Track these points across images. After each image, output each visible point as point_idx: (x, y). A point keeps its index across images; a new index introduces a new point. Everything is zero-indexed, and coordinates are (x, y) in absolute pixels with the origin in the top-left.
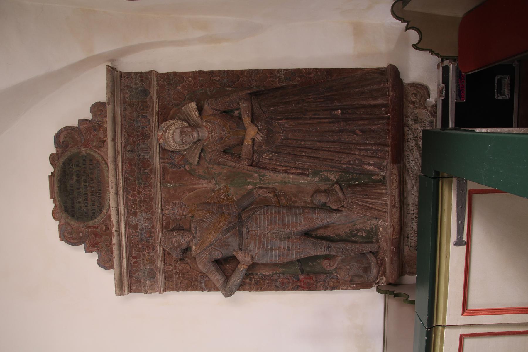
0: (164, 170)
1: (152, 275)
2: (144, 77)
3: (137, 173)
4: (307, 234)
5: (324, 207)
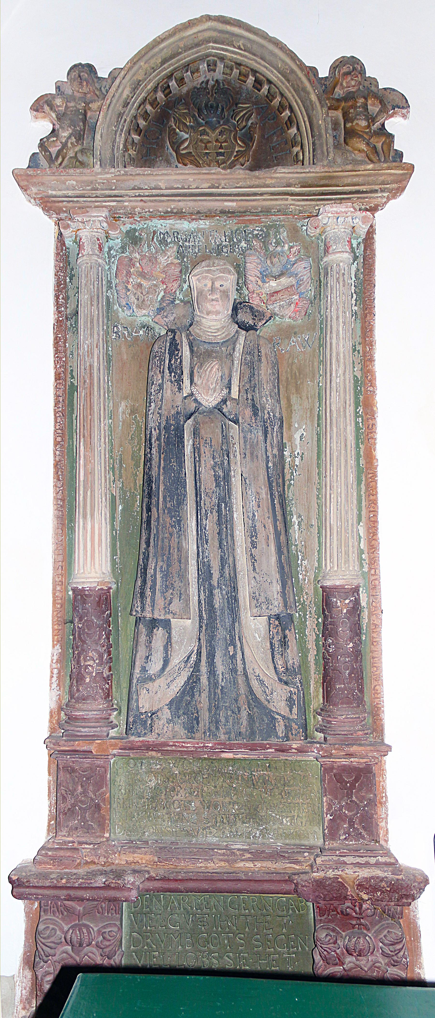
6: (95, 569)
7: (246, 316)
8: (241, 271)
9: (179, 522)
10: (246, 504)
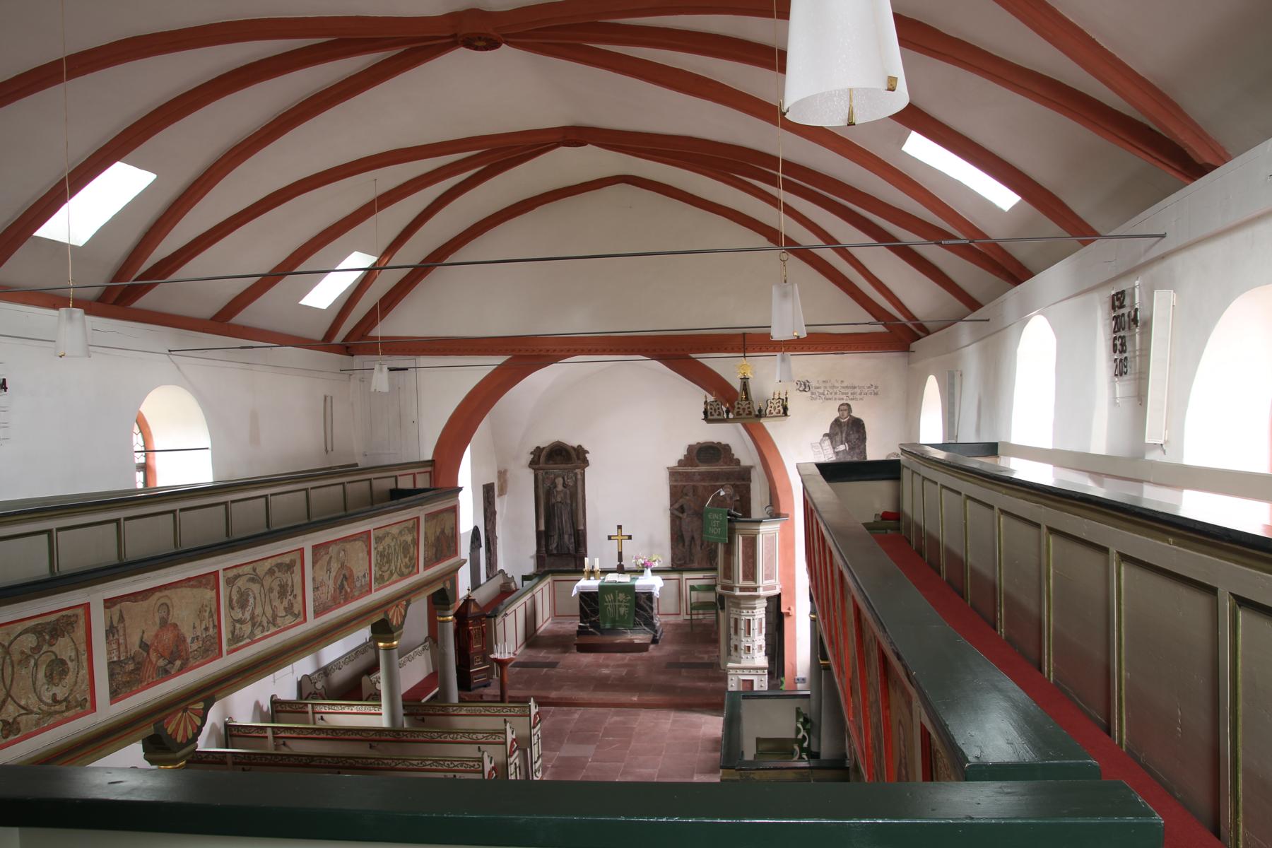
2: (749, 479)
3: (714, 476)
4: (693, 538)
6: (542, 528)
7: (565, 485)
10: (565, 517)
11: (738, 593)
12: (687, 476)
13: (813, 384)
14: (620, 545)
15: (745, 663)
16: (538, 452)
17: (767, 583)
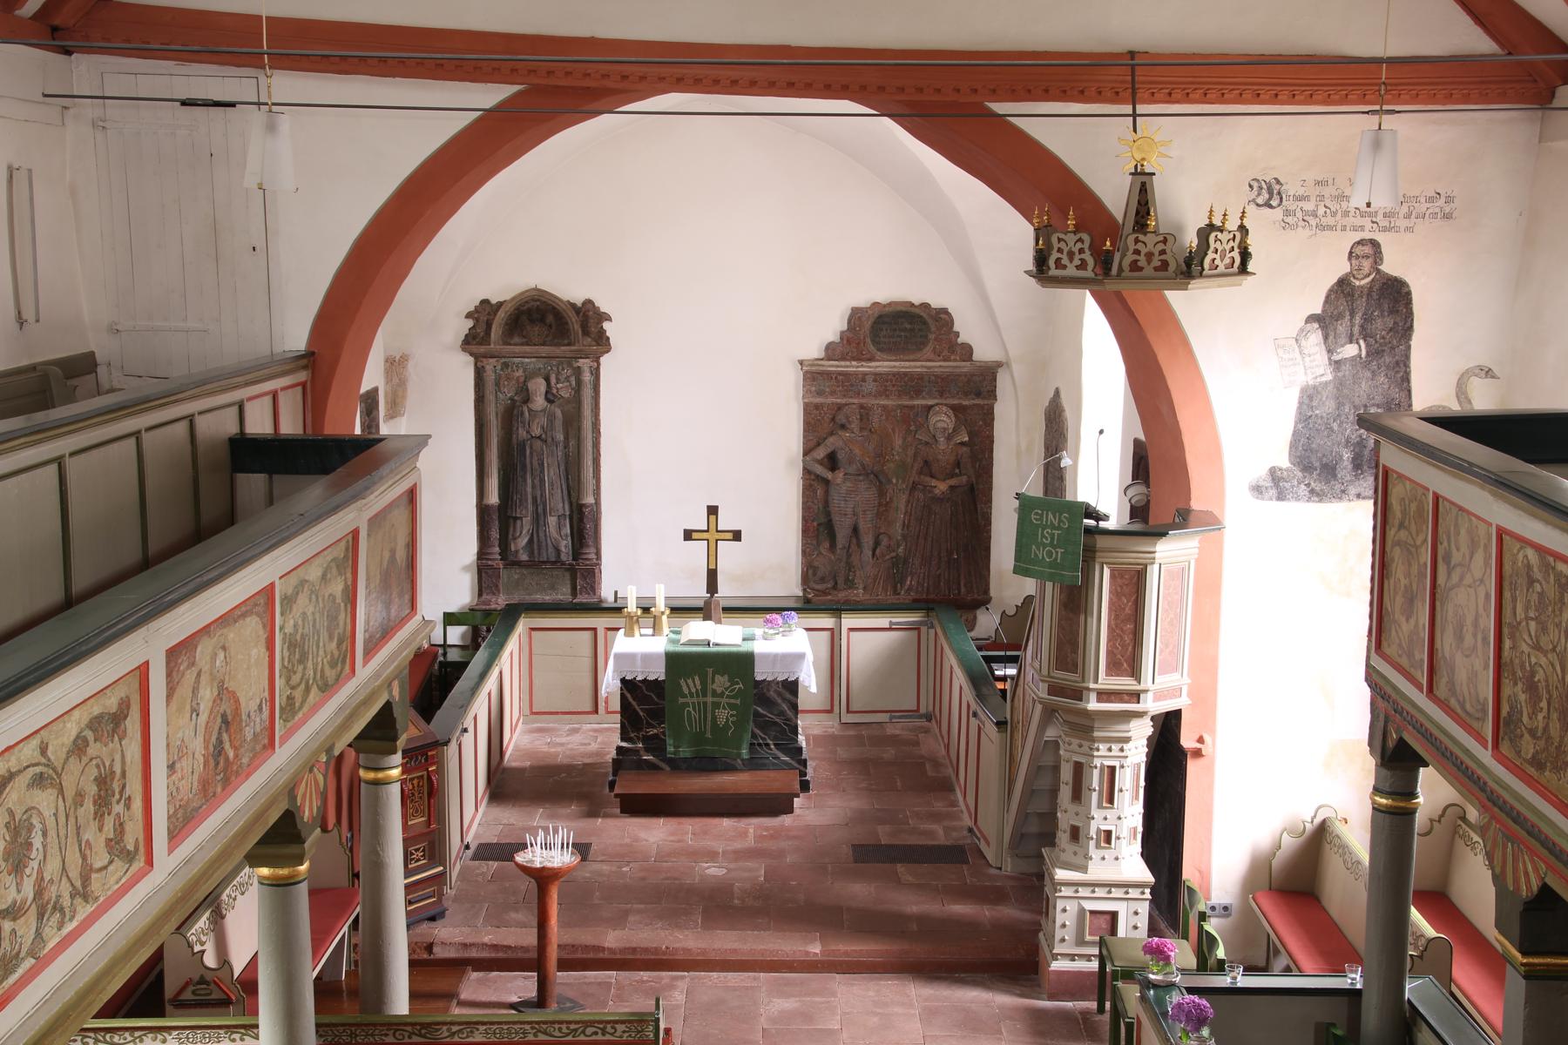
0: (912, 407)
1: (820, 393)
2: (992, 394)
3: (911, 385)
4: (855, 530)
5: (877, 543)
6: (493, 498)
7: (550, 397)
8: (547, 380)
9: (525, 480)
10: (552, 474)
11: (1093, 705)
12: (846, 382)
13: (1291, 188)
14: (712, 554)
15: (1098, 870)
16: (484, 312)
17: (1164, 681)
